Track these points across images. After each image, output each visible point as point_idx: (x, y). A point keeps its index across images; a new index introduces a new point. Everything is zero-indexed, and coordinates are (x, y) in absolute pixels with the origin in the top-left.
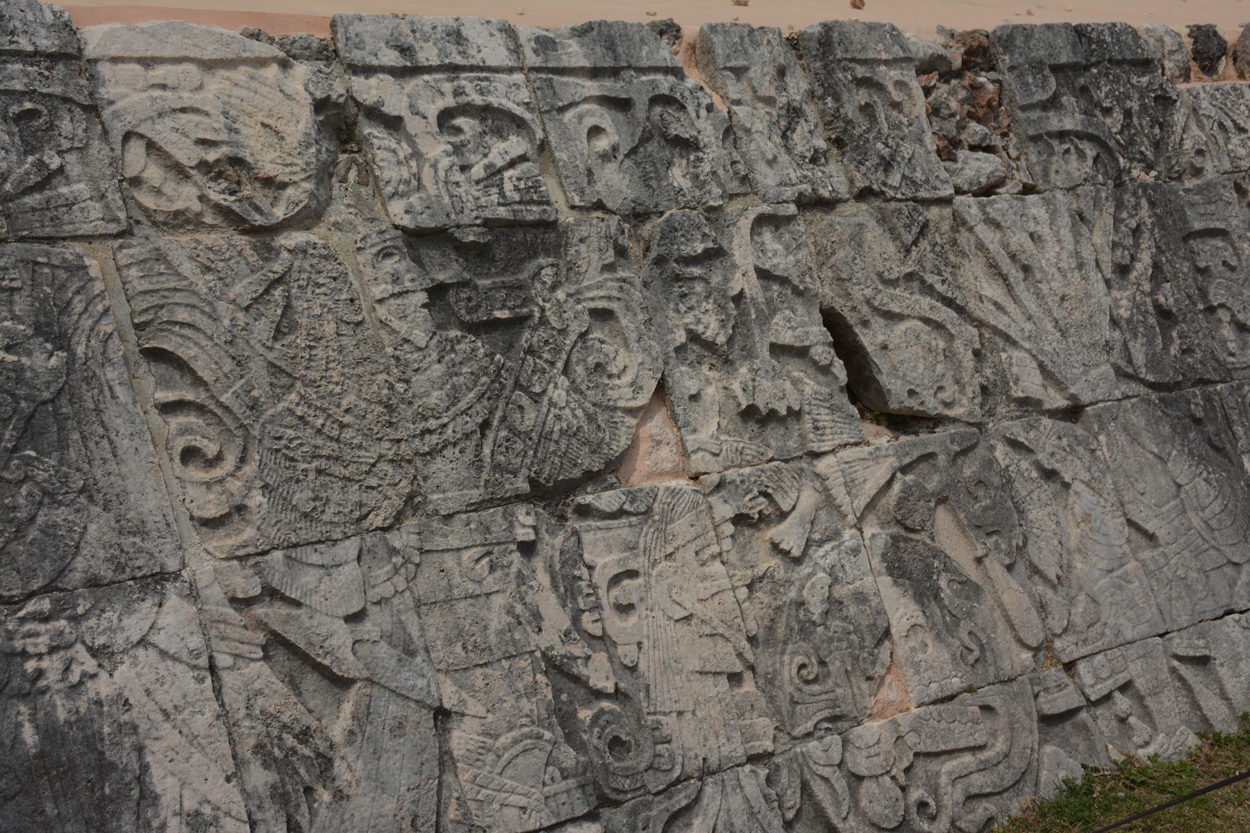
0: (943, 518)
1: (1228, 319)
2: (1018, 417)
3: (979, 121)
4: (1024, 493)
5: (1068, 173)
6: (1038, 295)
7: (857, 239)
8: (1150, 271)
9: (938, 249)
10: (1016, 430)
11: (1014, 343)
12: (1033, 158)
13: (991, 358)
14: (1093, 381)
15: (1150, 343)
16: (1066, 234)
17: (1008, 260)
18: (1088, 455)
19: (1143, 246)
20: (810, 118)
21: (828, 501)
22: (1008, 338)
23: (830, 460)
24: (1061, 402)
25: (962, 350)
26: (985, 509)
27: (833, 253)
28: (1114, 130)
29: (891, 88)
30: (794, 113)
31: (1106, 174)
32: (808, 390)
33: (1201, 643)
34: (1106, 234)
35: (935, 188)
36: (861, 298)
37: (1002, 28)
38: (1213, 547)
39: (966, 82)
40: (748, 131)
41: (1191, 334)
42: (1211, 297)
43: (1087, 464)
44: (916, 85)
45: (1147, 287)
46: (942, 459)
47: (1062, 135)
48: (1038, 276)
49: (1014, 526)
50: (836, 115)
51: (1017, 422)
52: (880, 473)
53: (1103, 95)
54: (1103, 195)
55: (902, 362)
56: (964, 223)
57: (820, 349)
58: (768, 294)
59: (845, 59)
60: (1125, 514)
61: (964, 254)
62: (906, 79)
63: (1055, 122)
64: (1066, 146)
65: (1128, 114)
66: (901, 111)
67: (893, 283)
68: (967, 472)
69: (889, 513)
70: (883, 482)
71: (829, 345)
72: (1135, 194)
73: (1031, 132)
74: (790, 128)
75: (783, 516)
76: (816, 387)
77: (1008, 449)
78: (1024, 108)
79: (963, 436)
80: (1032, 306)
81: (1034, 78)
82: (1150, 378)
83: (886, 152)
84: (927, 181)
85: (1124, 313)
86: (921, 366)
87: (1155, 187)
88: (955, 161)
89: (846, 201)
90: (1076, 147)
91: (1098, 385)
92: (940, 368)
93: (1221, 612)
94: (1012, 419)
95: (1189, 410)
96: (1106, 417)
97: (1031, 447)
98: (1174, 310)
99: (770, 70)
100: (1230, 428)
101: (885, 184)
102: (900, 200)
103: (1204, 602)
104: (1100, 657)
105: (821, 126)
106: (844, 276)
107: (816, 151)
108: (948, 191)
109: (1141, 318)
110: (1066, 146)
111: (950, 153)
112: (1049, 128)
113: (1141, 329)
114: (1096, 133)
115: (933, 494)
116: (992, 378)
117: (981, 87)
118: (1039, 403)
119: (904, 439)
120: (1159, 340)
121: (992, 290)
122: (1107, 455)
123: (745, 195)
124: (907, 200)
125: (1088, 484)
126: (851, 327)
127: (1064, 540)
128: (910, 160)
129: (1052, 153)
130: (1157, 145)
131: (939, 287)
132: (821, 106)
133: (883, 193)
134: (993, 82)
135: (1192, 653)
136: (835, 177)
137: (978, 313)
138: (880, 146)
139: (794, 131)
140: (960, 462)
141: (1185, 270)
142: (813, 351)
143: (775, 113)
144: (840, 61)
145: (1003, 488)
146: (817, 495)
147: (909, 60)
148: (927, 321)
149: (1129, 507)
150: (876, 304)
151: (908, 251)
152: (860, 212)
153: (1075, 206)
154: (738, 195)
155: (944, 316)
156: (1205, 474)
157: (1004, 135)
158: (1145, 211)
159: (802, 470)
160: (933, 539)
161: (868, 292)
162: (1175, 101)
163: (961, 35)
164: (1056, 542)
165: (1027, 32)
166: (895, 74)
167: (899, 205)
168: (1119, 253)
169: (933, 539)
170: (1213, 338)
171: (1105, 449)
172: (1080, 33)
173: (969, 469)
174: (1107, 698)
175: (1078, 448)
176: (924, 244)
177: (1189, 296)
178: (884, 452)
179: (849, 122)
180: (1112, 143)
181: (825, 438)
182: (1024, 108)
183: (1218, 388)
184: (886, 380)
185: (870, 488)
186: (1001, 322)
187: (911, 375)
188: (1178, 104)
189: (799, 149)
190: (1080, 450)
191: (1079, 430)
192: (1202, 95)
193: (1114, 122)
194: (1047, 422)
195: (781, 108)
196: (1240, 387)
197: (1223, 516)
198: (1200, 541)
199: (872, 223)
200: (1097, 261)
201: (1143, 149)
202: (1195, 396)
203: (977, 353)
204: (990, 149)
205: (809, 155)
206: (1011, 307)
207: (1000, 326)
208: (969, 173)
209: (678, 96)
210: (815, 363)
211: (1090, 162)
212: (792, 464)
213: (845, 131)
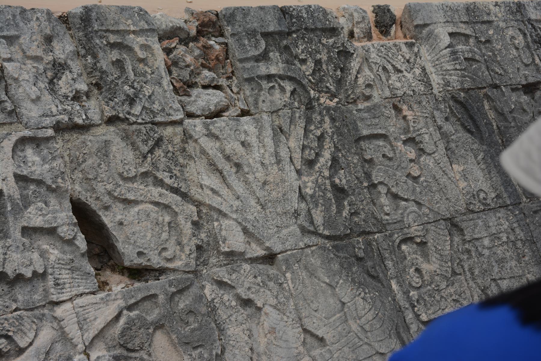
1: (385, 191)
2: (225, 265)
3: (210, 69)
4: (225, 317)
5: (272, 102)
6: (246, 182)
7: (104, 151)
9: (170, 155)
10: (223, 274)
11: (225, 215)
12: (248, 93)
13: (206, 226)
14: (284, 237)
15: (327, 209)
16: (269, 141)
17: (223, 160)
18: (276, 287)
19: (326, 147)
20: (74, 70)
21: (63, 336)
22: (220, 212)
23: (68, 306)
24: (260, 252)
25: (183, 222)
26: (193, 330)
27: (84, 161)
28: (307, 73)
29: (137, 49)
30: (59, 68)
31: (300, 102)
32: (52, 258)
34: (298, 140)
35: (169, 115)
36: (103, 191)
37: (226, 9)
38: (366, 343)
39: (200, 45)
40: (16, 80)
41: (357, 202)
42: (373, 178)
43: (275, 293)
44: (157, 47)
45: (327, 173)
46: (161, 298)
47: (269, 77)
48: (246, 169)
49: (215, 341)
50: (94, 68)
51: (224, 268)
52: (110, 312)
53: (300, 51)
54: (297, 115)
55: (134, 233)
56: (191, 137)
57: (65, 228)
58: (25, 192)
59: (101, 30)
60: (302, 325)
61: (190, 157)
62: (149, 43)
63: (263, 69)
64: (271, 85)
65: (318, 63)
66: (146, 64)
67: (127, 179)
68: (181, 305)
69: (114, 339)
70: (110, 318)
71: (75, 225)
72: (320, 113)
73: (245, 76)
74: (57, 76)
75: (21, 351)
76: (60, 256)
77: (214, 287)
78: (241, 61)
79: (179, 281)
80: (240, 188)
81: (250, 41)
82: (326, 233)
83: (131, 92)
84: (163, 110)
85: (309, 191)
86: (149, 235)
87: (335, 109)
88: (189, 96)
89: (100, 125)
90: (279, 85)
91: (287, 240)
92: (165, 236)
94: (221, 266)
95: (355, 252)
96: (291, 261)
97: (233, 284)
98: (346, 187)
99: (38, 38)
100: (383, 262)
101: (129, 113)
102: (141, 124)
105: (85, 75)
106: (90, 176)
107: (77, 92)
108: (179, 116)
109: (321, 194)
110: (271, 85)
111: (185, 90)
112: (259, 73)
113: (321, 201)
114: (294, 75)
115: (152, 323)
116: (205, 240)
117: (211, 47)
118: (242, 254)
119: (137, 285)
120: (334, 208)
121: (210, 180)
122: (291, 286)
123: (11, 124)
124: (146, 123)
125: (275, 307)
126: (95, 211)
127: (255, 347)
128: (150, 97)
129: (261, 89)
130: (339, 82)
131: (168, 181)
132: (84, 62)
133: (127, 119)
134: (220, 44)
136: (95, 109)
137: (198, 197)
138: (126, 88)
139: (60, 78)
140: (176, 299)
141: (355, 161)
142: (59, 230)
143: (41, 67)
144: (97, 32)
145: (208, 314)
146: (55, 332)
147: (152, 30)
148: (157, 204)
149: (305, 321)
150: (116, 194)
151: (145, 157)
152: (110, 133)
153: (277, 123)
155: (170, 200)
156: (363, 294)
157: (229, 78)
158: (327, 125)
159: (43, 315)
160: (150, 355)
161: (109, 187)
162: (353, 54)
163: (197, 14)
164: (247, 349)
165: (245, 12)
166: (141, 40)
167: (139, 127)
168: (307, 152)
169: (150, 355)
170: (374, 204)
171: (290, 282)
172: (284, 11)
173: (183, 303)
175: (269, 283)
176: (159, 152)
177: (357, 178)
178: (113, 297)
179: (103, 72)
180: (305, 81)
181: (64, 291)
182: (241, 61)
183: (376, 237)
184: (120, 246)
185: (99, 324)
186: (215, 202)
187: (140, 242)
188: (355, 55)
189: (63, 91)
190: (271, 284)
191: (272, 271)
192: (372, 49)
193: (308, 68)
194: (246, 267)
195: (48, 64)
196: (391, 236)
197: (375, 322)
198: (357, 340)
199: (118, 139)
200: (291, 158)
201: (328, 85)
202: (358, 242)
203: (195, 224)
204: (217, 87)
205: (71, 95)
206: (224, 191)
207: (214, 205)
208: (201, 103)
210: (61, 238)
211: (288, 94)
212: (36, 312)
213: (101, 78)
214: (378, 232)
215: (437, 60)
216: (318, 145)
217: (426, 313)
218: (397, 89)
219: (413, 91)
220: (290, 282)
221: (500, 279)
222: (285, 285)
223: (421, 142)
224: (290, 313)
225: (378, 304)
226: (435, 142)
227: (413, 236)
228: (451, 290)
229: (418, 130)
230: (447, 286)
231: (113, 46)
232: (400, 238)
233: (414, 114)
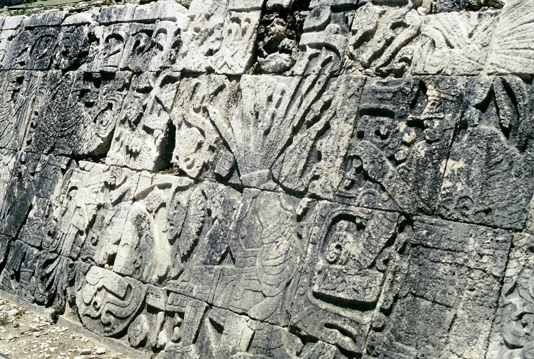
8: (322, 126)
45: (313, 136)
217: (320, 286)
222: (236, 211)
227: (355, 215)
228: (357, 279)
230: (357, 274)
233: (437, 95)
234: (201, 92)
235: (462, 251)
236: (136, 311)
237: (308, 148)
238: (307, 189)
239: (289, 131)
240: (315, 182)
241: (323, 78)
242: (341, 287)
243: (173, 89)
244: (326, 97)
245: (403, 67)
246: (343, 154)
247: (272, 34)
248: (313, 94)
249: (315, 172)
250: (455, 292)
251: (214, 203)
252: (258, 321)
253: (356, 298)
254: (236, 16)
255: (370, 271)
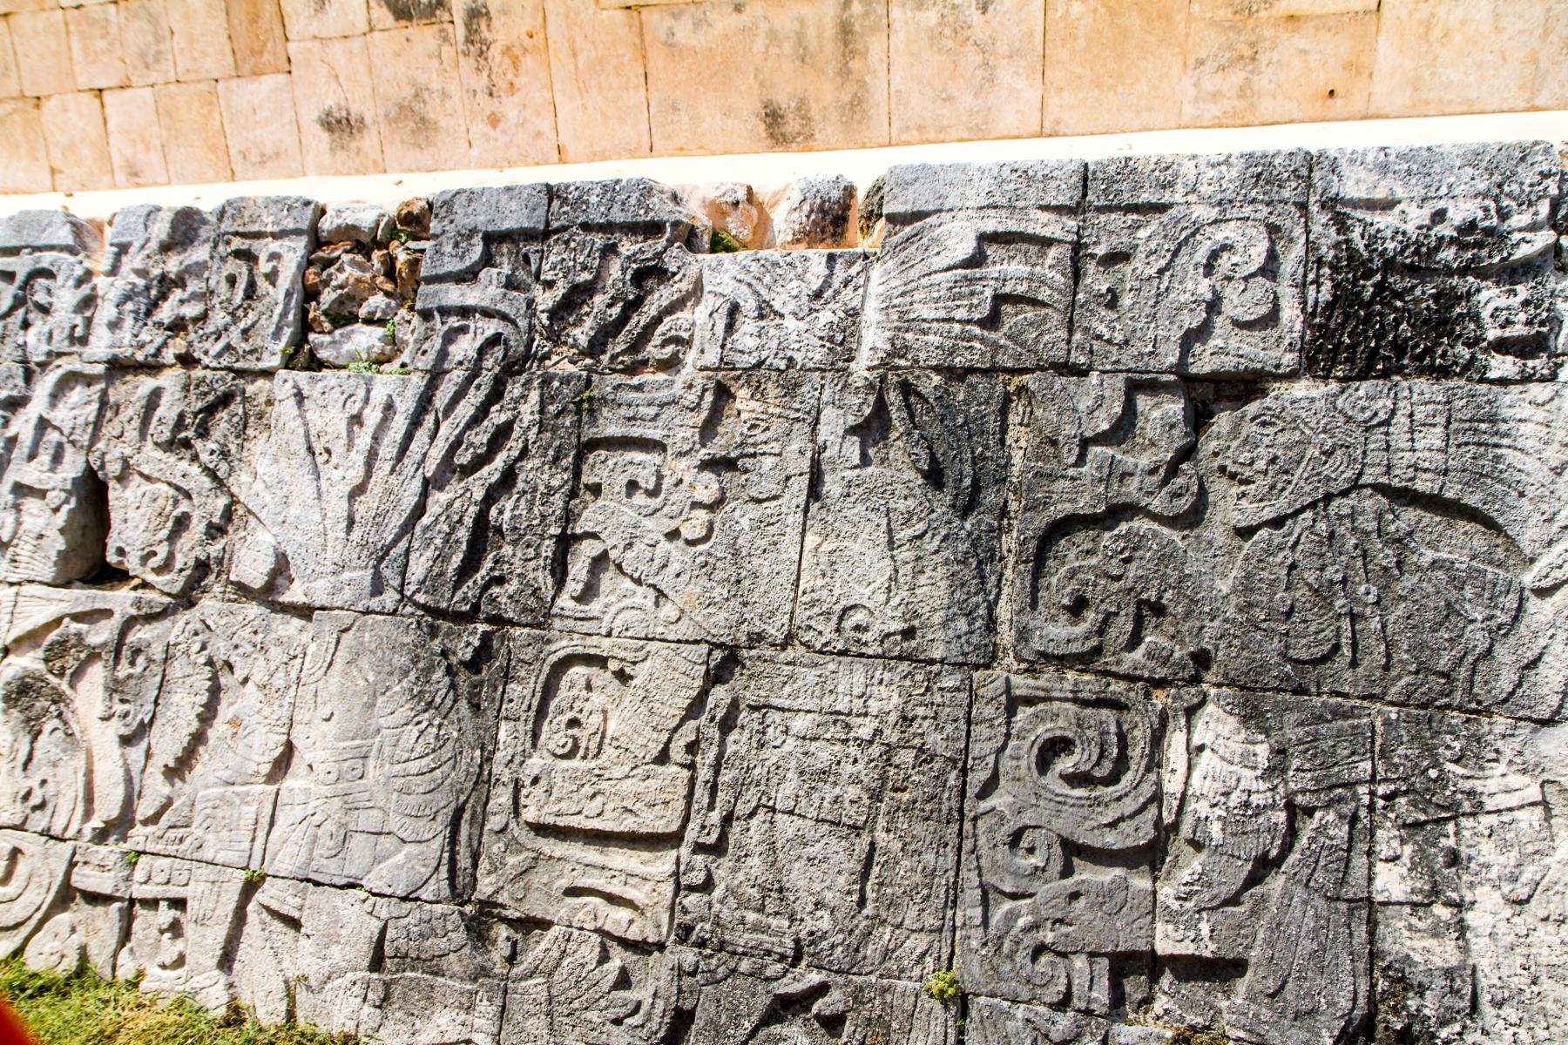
0: (97, 674)
8: (497, 476)
9: (236, 419)
15: (442, 558)
28: (540, 308)
33: (298, 901)
41: (516, 561)
45: (479, 494)
47: (465, 312)
81: (456, 245)
82: (421, 598)
86: (142, 527)
93: (344, 881)
98: (505, 526)
103: (325, 862)
104: (164, 862)
120: (457, 560)
123: (70, 354)
135: (275, 906)
154: (64, 354)
155: (192, 485)
160: (72, 686)
161: (128, 451)
162: (674, 274)
166: (274, 246)
174: (152, 904)
175: (273, 649)
188: (677, 278)
203: (210, 525)
209: (54, 269)
214: (531, 626)
215: (902, 295)
216: (489, 441)
218: (742, 352)
219: (791, 359)
220: (308, 659)
221: (791, 813)
223: (746, 471)
224: (281, 706)
225: (447, 752)
226: (788, 478)
229: (754, 445)
231: (238, 254)
232: (569, 651)
234: (167, 410)
235: (866, 715)
236: (44, 907)
237: (468, 521)
238: (476, 608)
239: (416, 485)
240: (496, 590)
241: (486, 379)
242: (593, 807)
243: (88, 403)
244: (498, 416)
245: (675, 354)
246: (555, 530)
247: (341, 287)
248: (465, 410)
249: (492, 569)
250: (865, 797)
251: (236, 647)
252: (394, 900)
253: (635, 827)
254: (245, 247)
255: (660, 769)
